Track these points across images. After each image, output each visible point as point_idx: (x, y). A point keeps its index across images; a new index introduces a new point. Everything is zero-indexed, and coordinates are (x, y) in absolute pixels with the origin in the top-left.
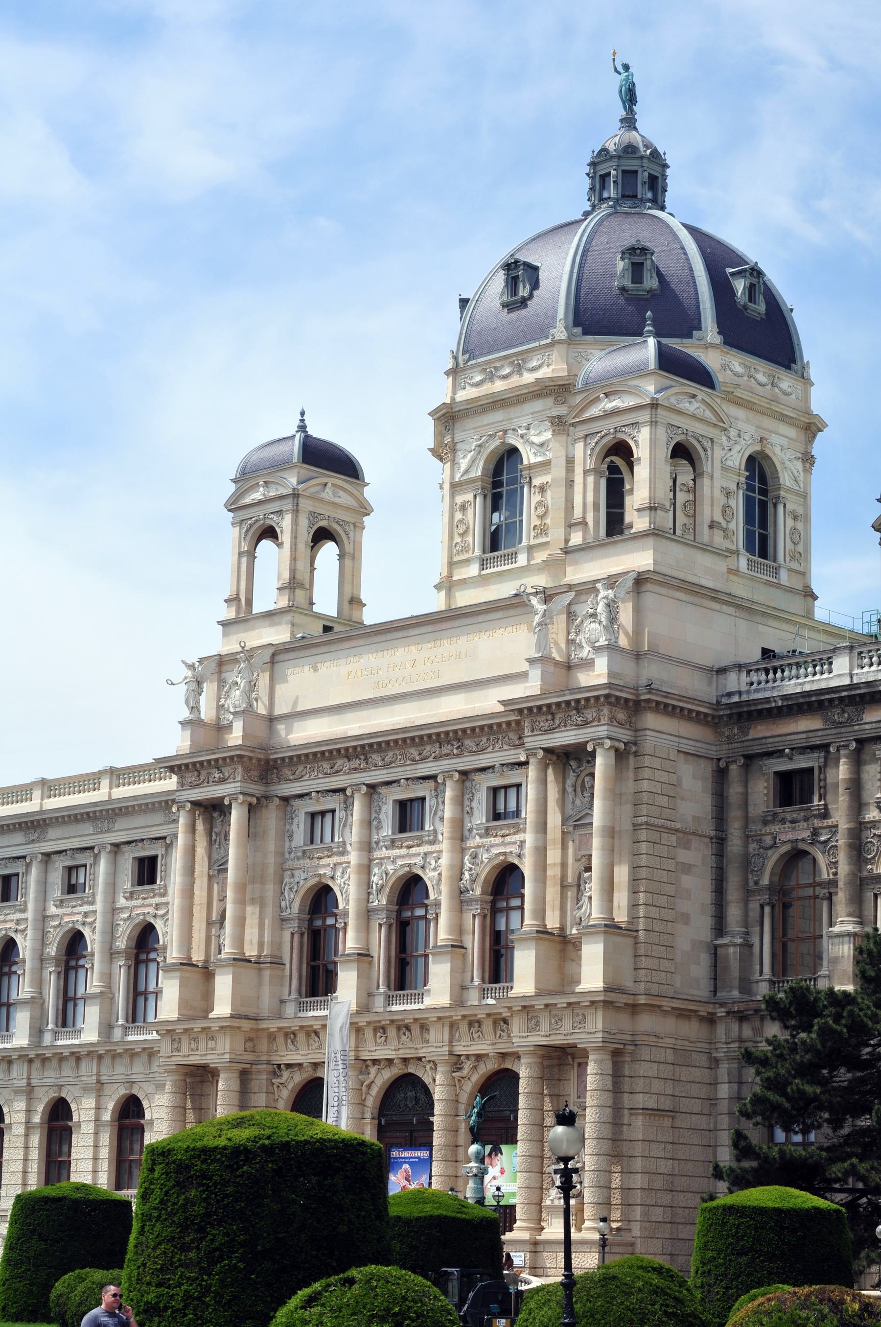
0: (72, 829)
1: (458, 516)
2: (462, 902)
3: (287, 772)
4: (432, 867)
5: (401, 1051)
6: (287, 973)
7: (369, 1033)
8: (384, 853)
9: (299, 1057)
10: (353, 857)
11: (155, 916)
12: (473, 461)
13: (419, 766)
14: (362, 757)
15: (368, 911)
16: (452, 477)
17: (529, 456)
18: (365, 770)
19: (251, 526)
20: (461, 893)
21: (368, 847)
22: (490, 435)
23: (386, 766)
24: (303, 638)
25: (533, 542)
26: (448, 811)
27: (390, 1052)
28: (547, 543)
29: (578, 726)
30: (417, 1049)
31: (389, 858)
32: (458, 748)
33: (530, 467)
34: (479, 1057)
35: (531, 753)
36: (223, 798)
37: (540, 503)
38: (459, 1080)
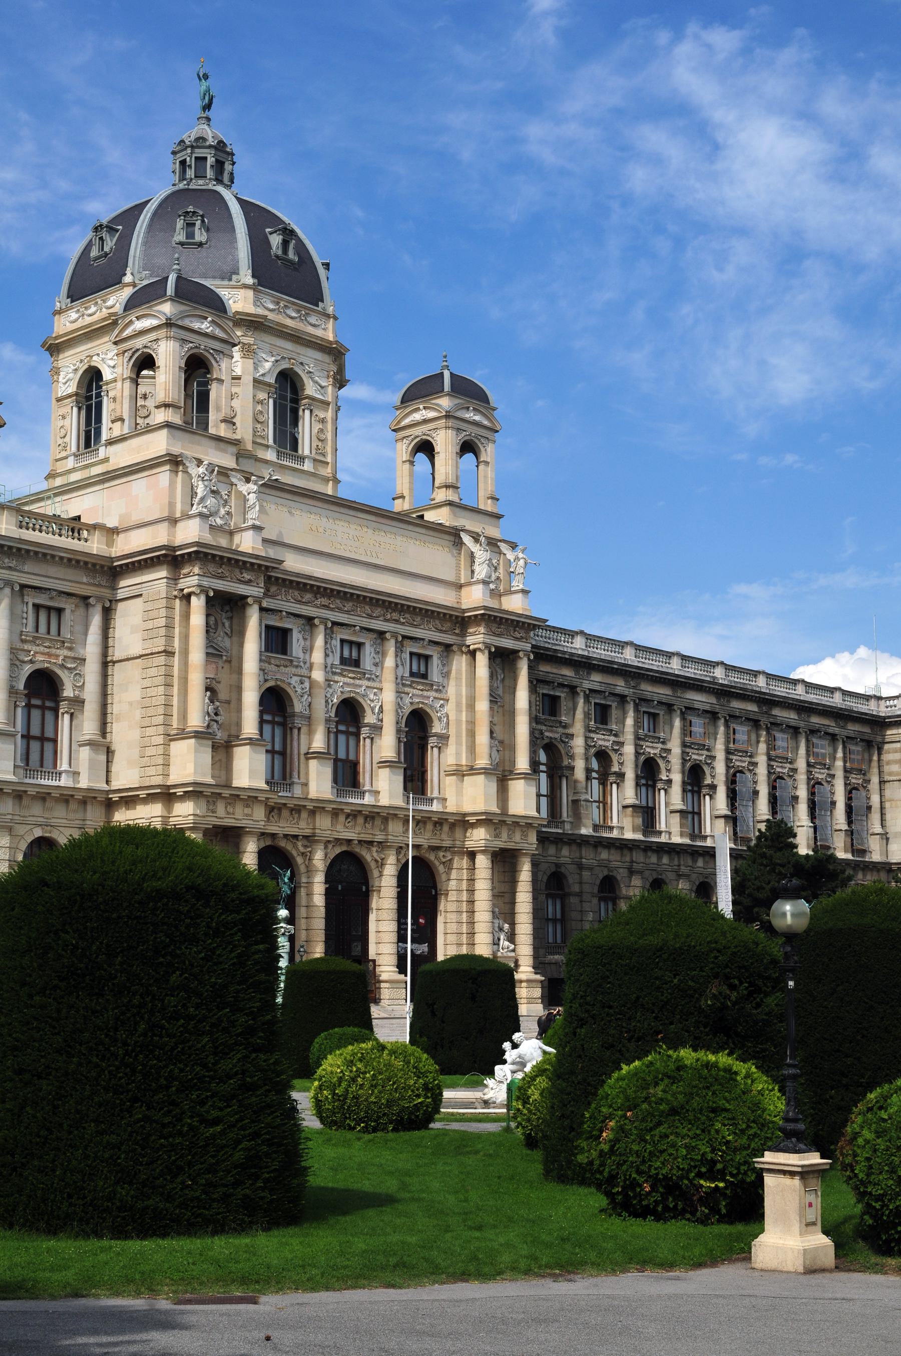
0: (70, 574)
5: (362, 835)
7: (342, 818)
9: (277, 828)
13: (373, 621)
17: (310, 389)
18: (332, 610)
19: (192, 348)
23: (347, 612)
24: (276, 480)
25: (313, 455)
27: (353, 835)
28: (328, 463)
29: (517, 639)
35: (487, 646)
36: (248, 597)
37: (321, 431)
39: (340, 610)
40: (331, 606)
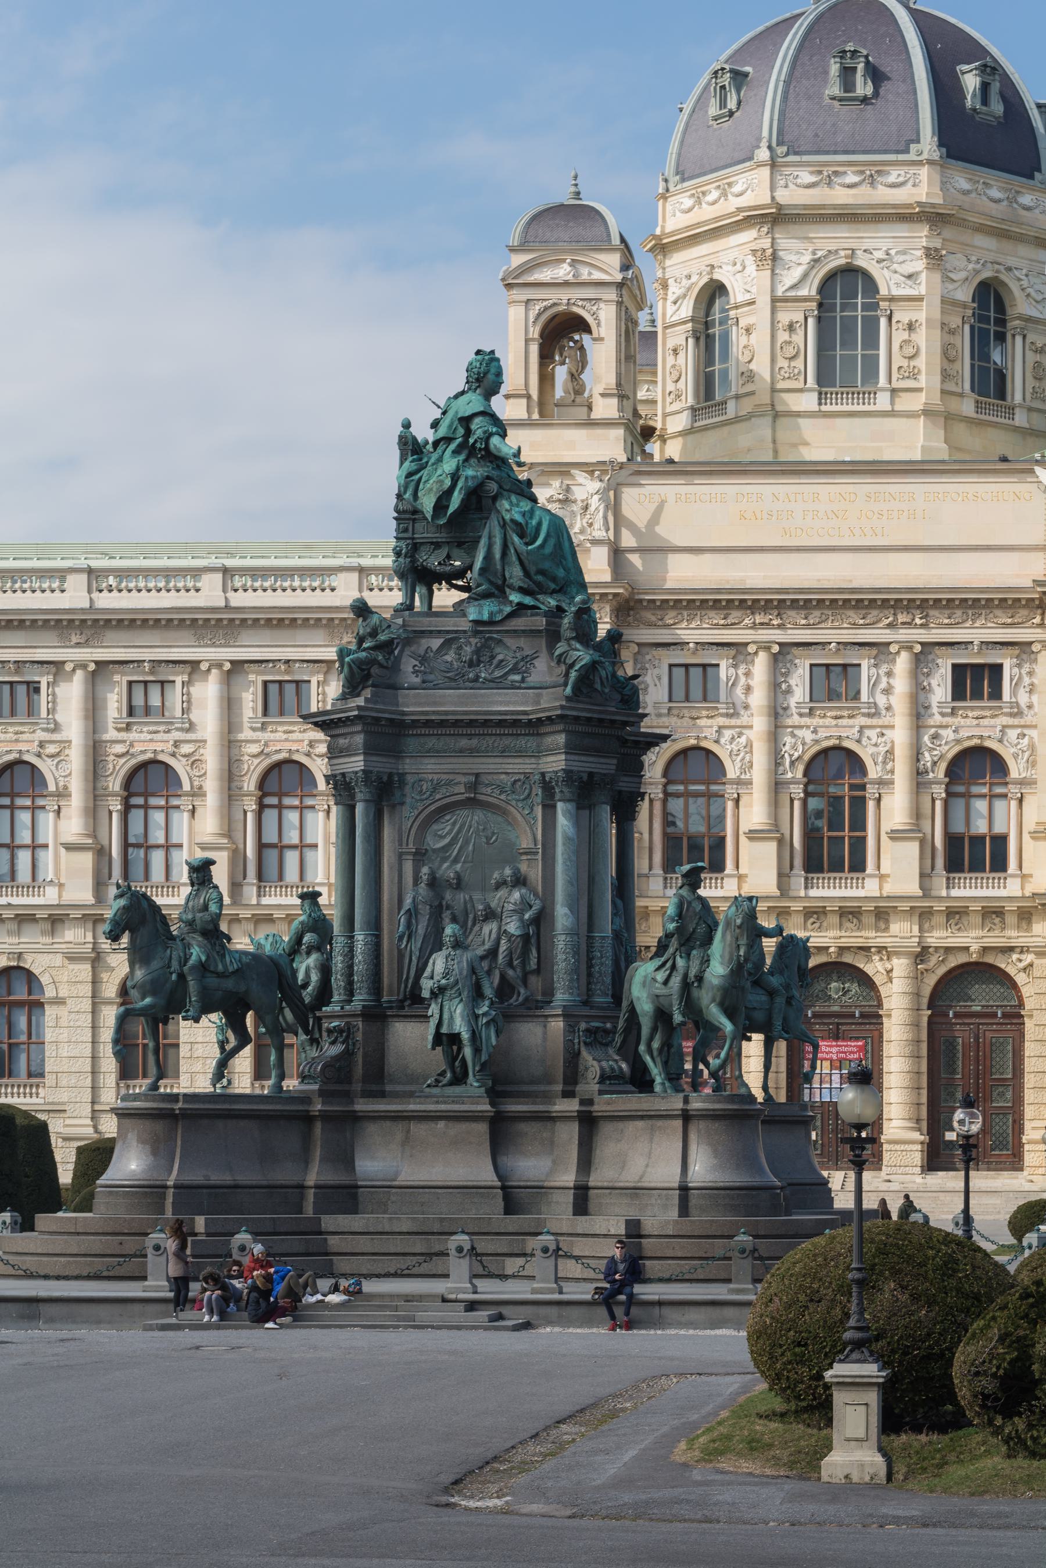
1: (783, 336)
2: (918, 784)
3: (649, 616)
4: (874, 741)
5: (843, 940)
6: (647, 844)
8: (795, 720)
10: (759, 724)
11: (308, 755)
12: (805, 276)
14: (776, 613)
15: (776, 784)
16: (773, 290)
20: (918, 773)
21: (776, 713)
22: (829, 251)
25: (895, 384)
26: (901, 684)
28: (920, 390)
30: (867, 938)
31: (808, 727)
32: (921, 618)
33: (892, 299)
34: (948, 950)
38: (922, 973)
39: (797, 626)
40: (775, 622)
